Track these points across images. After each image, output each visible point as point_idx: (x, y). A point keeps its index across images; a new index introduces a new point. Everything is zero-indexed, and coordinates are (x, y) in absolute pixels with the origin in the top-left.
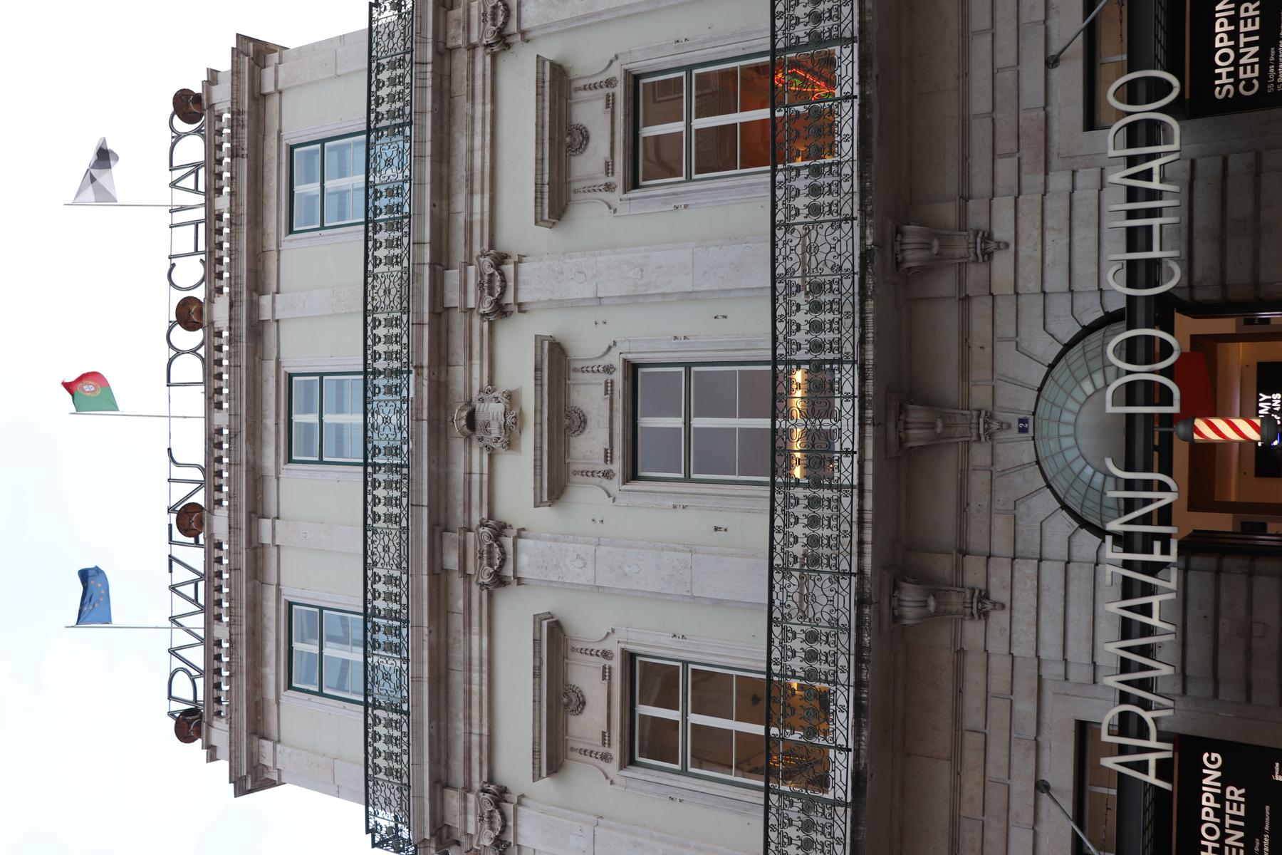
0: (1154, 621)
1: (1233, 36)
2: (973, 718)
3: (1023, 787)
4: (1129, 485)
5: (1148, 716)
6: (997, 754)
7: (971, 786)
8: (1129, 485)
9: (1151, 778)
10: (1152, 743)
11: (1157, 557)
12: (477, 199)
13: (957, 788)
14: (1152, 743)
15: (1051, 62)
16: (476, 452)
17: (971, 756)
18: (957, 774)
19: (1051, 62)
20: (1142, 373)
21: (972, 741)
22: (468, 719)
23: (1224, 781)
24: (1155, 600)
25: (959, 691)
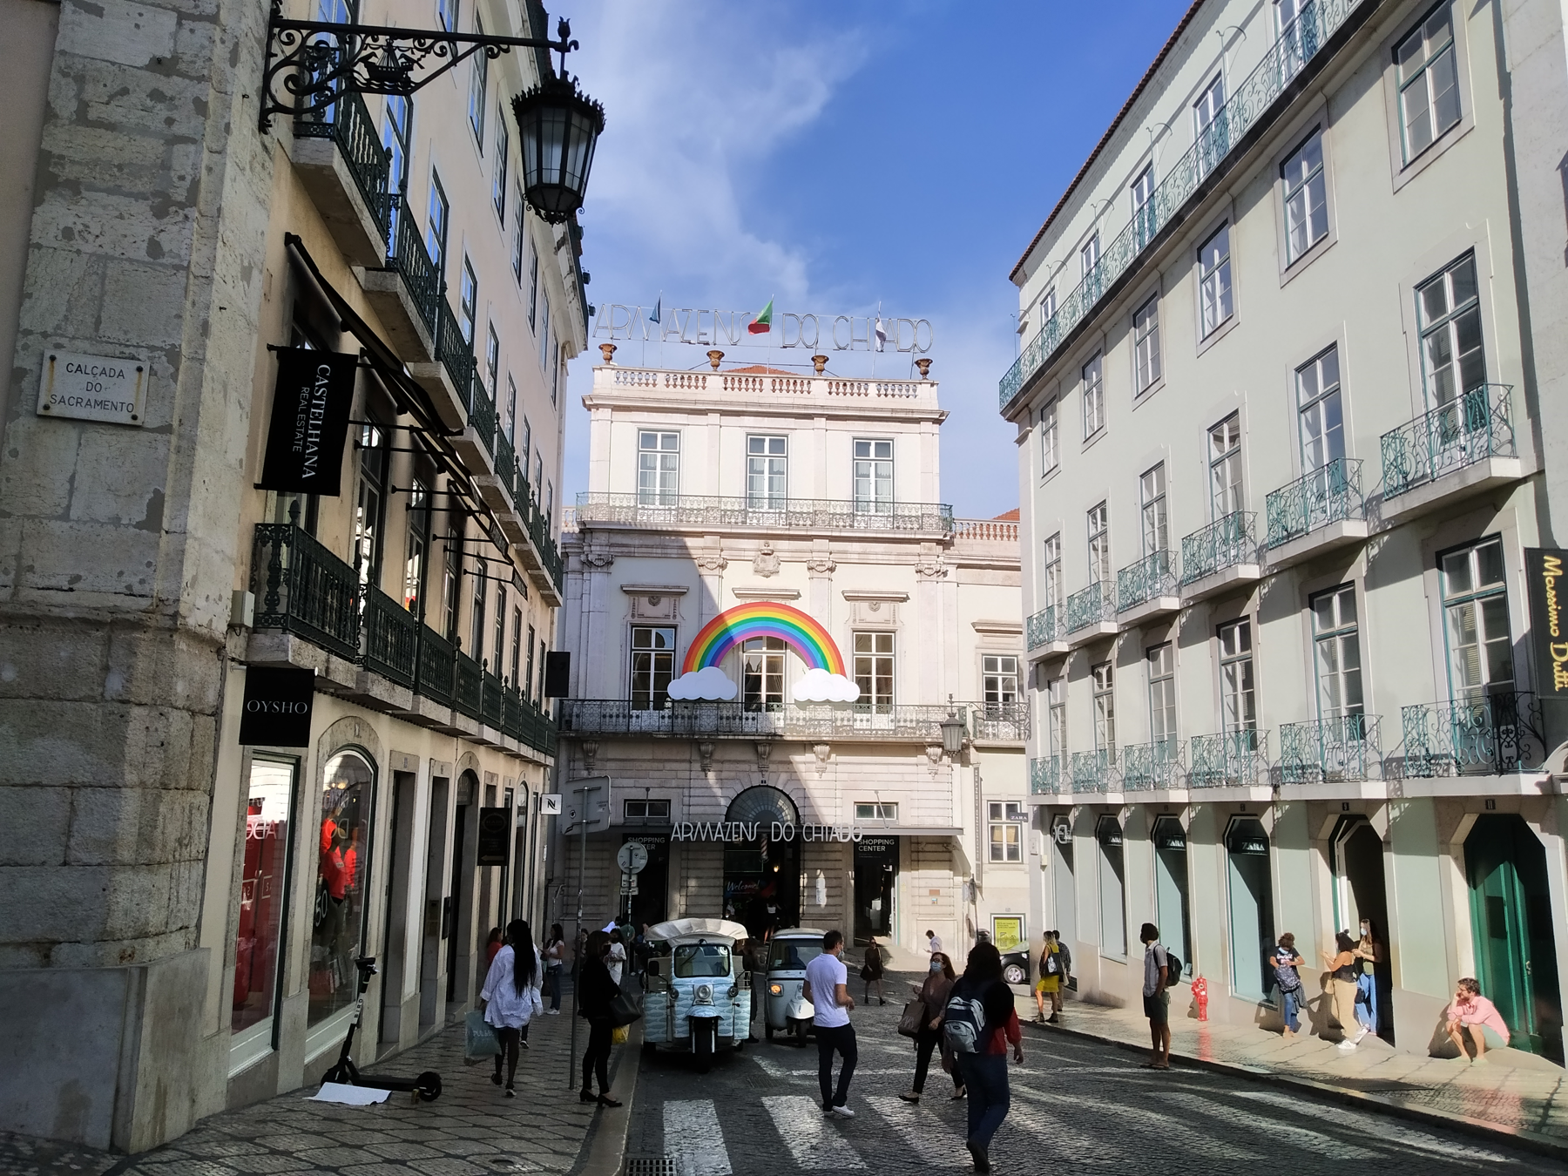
0: (716, 836)
1: (877, 844)
2: (668, 766)
3: (647, 783)
4: (753, 828)
5: (690, 834)
6: (657, 774)
7: (645, 765)
8: (753, 828)
9: (673, 836)
10: (683, 836)
11: (734, 836)
12: (856, 556)
13: (644, 760)
14: (683, 836)
15: (876, 792)
16: (753, 553)
17: (655, 765)
18: (649, 760)
19: (876, 792)
20: (783, 831)
21: (660, 766)
22: (641, 546)
23: (656, 844)
24: (722, 836)
25: (676, 761)
